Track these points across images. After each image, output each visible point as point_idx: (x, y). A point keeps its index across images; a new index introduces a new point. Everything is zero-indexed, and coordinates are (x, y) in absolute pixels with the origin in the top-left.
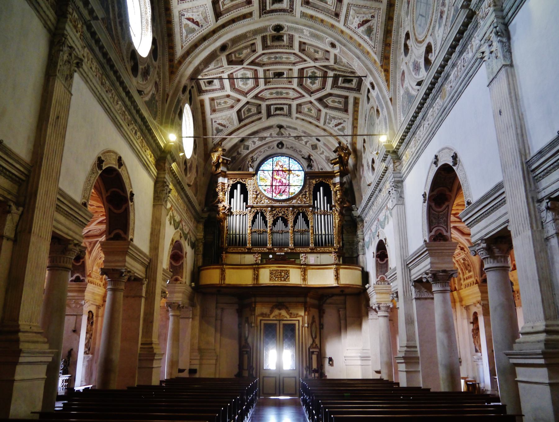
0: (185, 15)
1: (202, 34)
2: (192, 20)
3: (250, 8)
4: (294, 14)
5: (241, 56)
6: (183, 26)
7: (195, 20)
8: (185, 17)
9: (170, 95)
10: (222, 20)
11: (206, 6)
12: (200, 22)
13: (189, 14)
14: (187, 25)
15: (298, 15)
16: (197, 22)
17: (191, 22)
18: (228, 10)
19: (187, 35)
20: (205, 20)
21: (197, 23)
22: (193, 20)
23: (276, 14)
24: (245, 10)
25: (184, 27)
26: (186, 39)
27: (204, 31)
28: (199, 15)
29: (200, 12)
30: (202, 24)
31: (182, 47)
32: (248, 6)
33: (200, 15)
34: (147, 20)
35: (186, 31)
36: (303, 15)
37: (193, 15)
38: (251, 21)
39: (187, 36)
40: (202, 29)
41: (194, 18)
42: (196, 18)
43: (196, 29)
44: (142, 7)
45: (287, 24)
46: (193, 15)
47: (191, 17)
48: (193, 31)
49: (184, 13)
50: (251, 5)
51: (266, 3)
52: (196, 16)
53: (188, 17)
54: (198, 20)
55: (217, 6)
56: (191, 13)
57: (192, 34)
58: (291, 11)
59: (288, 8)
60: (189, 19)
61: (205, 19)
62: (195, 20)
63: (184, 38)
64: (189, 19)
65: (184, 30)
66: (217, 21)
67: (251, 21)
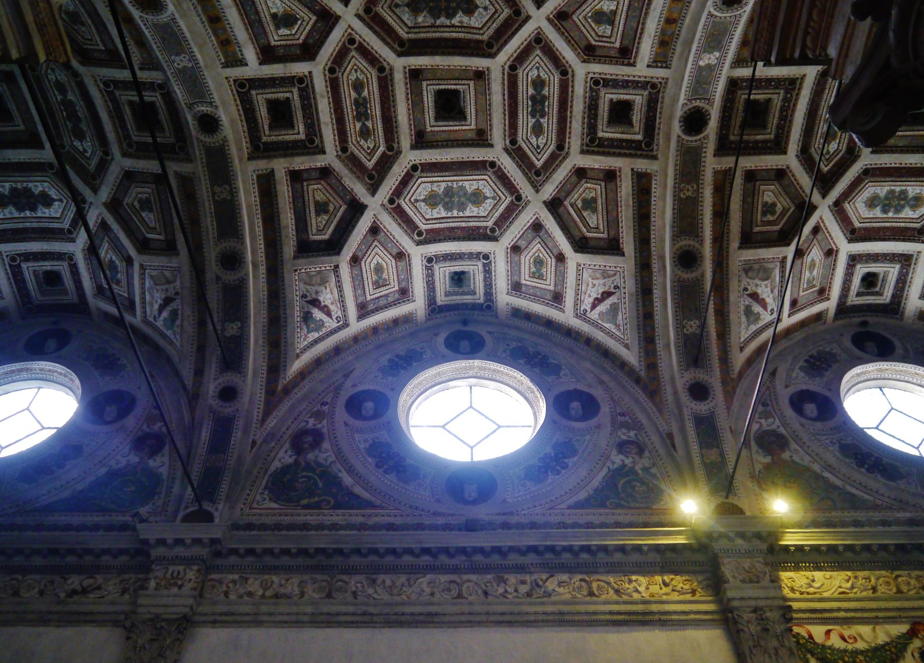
0: (587, 308)
1: (630, 294)
2: (597, 302)
3: (623, 176)
4: (660, 80)
5: (779, 208)
6: (600, 322)
7: (599, 296)
8: (589, 310)
9: (675, 430)
10: (628, 243)
11: (582, 266)
12: (606, 289)
13: (586, 302)
14: (601, 314)
15: (660, 73)
16: (603, 293)
17: (598, 304)
18: (613, 222)
19: (616, 324)
20: (609, 276)
21: (606, 295)
22: (596, 299)
23: (658, 120)
24: (626, 188)
25: (602, 321)
26: (620, 330)
27: (629, 285)
28: (594, 285)
29: (590, 279)
30: (613, 286)
31: (627, 346)
32: (618, 180)
33: (595, 282)
34: (529, 388)
35: (609, 321)
36: (661, 60)
37: (590, 296)
38: (658, 178)
39: (618, 326)
40: (623, 291)
41: (595, 296)
42: (595, 293)
43: (616, 301)
44: (511, 383)
45: (682, 99)
46: (590, 296)
47: (591, 300)
48: (614, 308)
49: (582, 309)
50: (618, 174)
51: (622, 140)
52: (593, 290)
53: (590, 306)
54: (601, 291)
55: (592, 243)
56: (587, 296)
57: (620, 314)
58: (654, 86)
59: (646, 93)
60: (594, 307)
61: (605, 275)
62: (599, 296)
63: (618, 333)
64: (594, 307)
65: (607, 325)
66: (623, 255)
67: (658, 178)
